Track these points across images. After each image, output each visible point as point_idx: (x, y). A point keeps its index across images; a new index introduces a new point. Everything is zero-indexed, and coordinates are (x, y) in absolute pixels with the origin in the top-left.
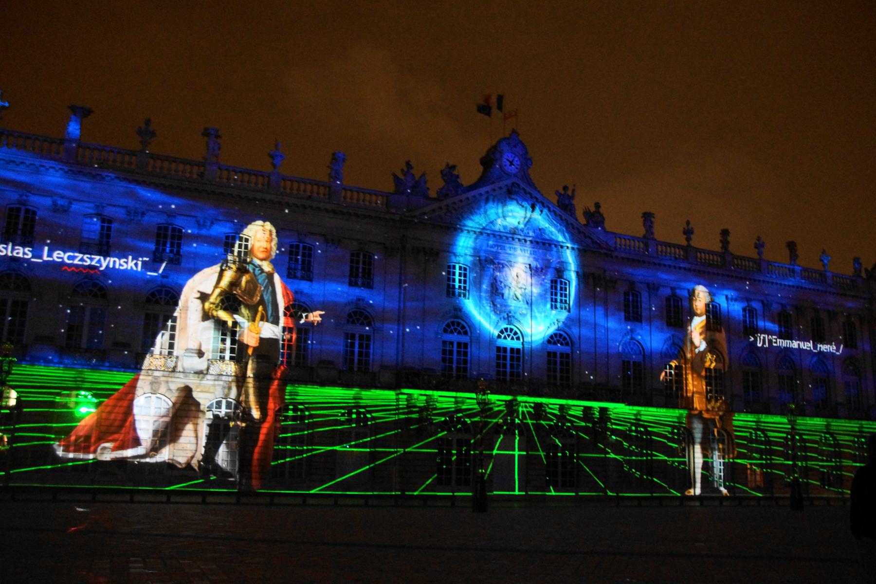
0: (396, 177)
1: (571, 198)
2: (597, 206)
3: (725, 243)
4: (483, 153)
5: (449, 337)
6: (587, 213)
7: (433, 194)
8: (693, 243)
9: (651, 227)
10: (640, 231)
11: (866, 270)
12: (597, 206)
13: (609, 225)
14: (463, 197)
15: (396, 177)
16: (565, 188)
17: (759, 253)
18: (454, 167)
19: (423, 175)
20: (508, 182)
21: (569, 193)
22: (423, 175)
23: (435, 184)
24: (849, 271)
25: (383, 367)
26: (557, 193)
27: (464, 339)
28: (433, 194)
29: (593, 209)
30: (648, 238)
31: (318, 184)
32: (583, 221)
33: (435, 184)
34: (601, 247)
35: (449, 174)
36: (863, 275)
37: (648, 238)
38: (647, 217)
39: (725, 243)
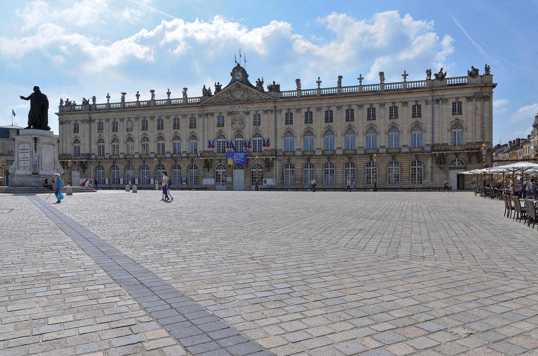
2: (274, 82)
5: (219, 140)
6: (270, 88)
10: (295, 88)
11: (436, 75)
12: (274, 82)
16: (259, 79)
24: (424, 77)
26: (257, 82)
28: (213, 94)
29: (272, 84)
32: (266, 90)
36: (433, 77)
37: (299, 90)
38: (298, 81)
39: (339, 82)
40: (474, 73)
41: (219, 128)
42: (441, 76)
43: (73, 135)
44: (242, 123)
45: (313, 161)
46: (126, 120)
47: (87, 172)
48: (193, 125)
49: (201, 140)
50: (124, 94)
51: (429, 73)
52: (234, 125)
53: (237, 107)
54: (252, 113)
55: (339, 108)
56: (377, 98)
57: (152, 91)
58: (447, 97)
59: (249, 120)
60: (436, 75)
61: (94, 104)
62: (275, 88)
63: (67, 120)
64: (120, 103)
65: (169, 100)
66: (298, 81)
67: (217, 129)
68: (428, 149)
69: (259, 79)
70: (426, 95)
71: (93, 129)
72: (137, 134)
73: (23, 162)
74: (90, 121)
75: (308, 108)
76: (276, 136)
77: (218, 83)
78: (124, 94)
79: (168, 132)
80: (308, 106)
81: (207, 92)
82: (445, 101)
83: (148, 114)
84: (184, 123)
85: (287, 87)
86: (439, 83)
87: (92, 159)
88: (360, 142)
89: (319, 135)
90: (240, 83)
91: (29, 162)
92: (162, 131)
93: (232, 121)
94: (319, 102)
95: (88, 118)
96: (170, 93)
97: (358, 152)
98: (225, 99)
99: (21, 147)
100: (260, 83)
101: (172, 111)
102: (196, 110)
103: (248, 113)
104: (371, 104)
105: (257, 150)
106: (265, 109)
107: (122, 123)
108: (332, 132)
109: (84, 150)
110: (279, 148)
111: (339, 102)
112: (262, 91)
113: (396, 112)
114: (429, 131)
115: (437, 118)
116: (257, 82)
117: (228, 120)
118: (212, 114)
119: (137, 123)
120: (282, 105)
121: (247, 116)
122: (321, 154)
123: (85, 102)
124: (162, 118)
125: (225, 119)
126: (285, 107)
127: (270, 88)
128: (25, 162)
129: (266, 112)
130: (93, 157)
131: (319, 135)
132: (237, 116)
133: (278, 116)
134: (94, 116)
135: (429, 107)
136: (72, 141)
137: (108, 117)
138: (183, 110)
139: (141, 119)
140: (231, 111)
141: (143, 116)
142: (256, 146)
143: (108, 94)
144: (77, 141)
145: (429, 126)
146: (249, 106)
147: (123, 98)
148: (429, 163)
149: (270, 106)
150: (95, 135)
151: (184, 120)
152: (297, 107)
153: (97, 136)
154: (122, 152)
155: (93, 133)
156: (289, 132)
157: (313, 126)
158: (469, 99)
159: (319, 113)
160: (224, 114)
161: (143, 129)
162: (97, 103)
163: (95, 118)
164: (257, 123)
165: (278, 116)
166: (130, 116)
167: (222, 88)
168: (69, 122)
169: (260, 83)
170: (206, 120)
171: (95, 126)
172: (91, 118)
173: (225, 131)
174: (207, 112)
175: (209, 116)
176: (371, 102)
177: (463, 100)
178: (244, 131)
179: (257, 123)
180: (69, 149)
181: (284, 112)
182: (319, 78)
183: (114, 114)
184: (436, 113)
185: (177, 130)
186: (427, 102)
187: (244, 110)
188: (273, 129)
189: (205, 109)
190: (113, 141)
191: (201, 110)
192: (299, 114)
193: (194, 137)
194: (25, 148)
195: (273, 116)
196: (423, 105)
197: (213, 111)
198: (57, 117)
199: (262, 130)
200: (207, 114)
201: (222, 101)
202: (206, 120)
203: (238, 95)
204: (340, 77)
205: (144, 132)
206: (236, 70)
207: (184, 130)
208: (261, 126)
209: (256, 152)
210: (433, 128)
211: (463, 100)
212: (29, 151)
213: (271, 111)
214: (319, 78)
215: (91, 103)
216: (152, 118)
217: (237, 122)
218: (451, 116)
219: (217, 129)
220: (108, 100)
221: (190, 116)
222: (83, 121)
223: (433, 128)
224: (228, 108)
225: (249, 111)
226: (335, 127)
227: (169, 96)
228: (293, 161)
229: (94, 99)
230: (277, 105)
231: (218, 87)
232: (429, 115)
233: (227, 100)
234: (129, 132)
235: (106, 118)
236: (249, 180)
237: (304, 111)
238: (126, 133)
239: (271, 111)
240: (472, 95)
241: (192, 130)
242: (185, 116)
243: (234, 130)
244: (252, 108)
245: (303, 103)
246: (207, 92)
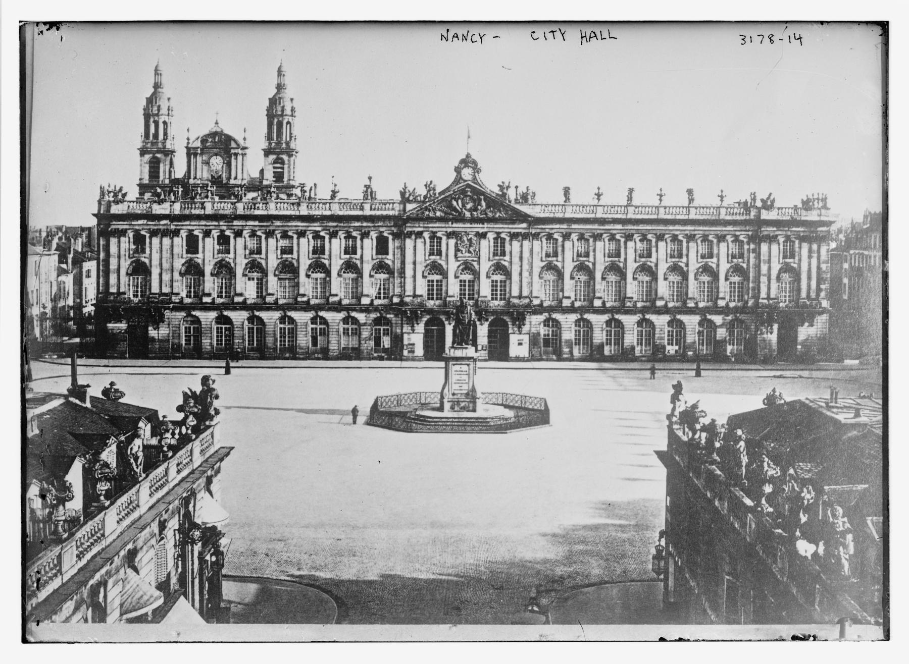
3: (630, 198)
11: (762, 200)
15: (401, 192)
39: (630, 198)
40: (807, 205)
52: (459, 254)
59: (486, 247)
60: (762, 200)
77: (431, 182)
116: (499, 186)
129: (514, 236)
149: (521, 227)
171: (180, 243)
182: (599, 188)
204: (631, 191)
214: (599, 188)
231: (429, 187)
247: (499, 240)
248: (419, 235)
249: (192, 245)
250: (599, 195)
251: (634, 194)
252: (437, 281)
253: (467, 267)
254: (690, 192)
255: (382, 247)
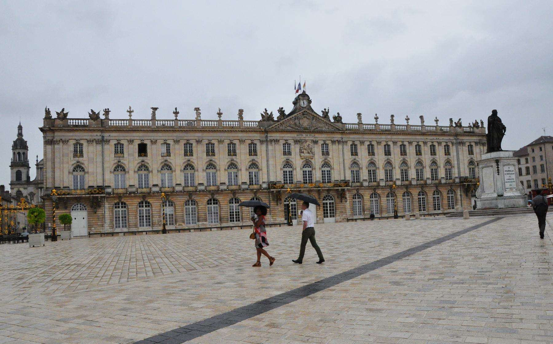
0: (262, 115)
1: (327, 113)
2: (338, 114)
3: (392, 120)
4: (293, 100)
6: (335, 118)
7: (275, 119)
8: (378, 123)
9: (361, 119)
10: (356, 121)
12: (338, 114)
13: (344, 121)
14: (286, 119)
15: (262, 115)
16: (325, 109)
17: (408, 123)
18: (282, 108)
19: (271, 113)
20: (303, 111)
21: (327, 111)
22: (271, 113)
23: (276, 115)
24: (448, 124)
25: (264, 182)
26: (322, 111)
27: (290, 169)
28: (275, 119)
29: (337, 115)
30: (360, 123)
31: (235, 121)
32: (332, 120)
33: (276, 115)
34: (339, 130)
35: (281, 111)
36: (454, 125)
37: (360, 123)
38: (359, 115)
39: (392, 120)
41: (286, 156)
42: (459, 125)
43: (73, 161)
44: (311, 152)
45: (379, 192)
46: (160, 142)
47: (100, 212)
48: (253, 151)
49: (265, 170)
50: (155, 109)
51: (451, 120)
52: (302, 155)
53: (304, 135)
54: (321, 142)
55: (395, 143)
56: (422, 137)
57: (197, 109)
58: (465, 141)
59: (317, 150)
61: (107, 119)
62: (338, 119)
63: (64, 138)
64: (150, 120)
65: (220, 121)
66: (359, 115)
67: (284, 158)
68: (457, 180)
69: (325, 109)
70: (452, 138)
71: (106, 152)
72: (178, 160)
73: (509, 184)
74: (103, 141)
75: (370, 142)
76: (344, 167)
77: (282, 108)
78: (155, 109)
79: (222, 159)
80: (370, 140)
81: (267, 117)
82: (462, 143)
83: (193, 137)
84: (242, 151)
85: (349, 119)
86: (459, 130)
87: (109, 194)
88: (223, 177)
89: (381, 167)
90: (308, 111)
91: (515, 183)
92: (213, 158)
93: (300, 150)
94: (379, 137)
95: (100, 138)
96: (222, 114)
97: (381, 184)
98: (292, 126)
99: (506, 168)
100: (326, 114)
101: (226, 134)
102: (257, 136)
103: (316, 142)
104: (418, 142)
105: (327, 181)
106: (332, 139)
107: (154, 146)
108: (257, 165)
109: (93, 179)
110: (347, 179)
111: (395, 138)
112: (330, 121)
113: (373, 150)
114: (456, 166)
115: (461, 156)
116: (322, 111)
117: (295, 149)
118: (277, 141)
119: (177, 146)
120: (348, 136)
121: (316, 146)
122: (384, 184)
123: (94, 116)
124: (213, 142)
125: (292, 147)
126: (351, 139)
127: (335, 118)
128: (511, 183)
129: (333, 142)
130: (109, 190)
131: (381, 167)
132: (306, 145)
133: (345, 146)
134: (106, 135)
135: (454, 147)
136: (72, 168)
137: (132, 138)
138: (240, 135)
139: (182, 143)
140: (299, 139)
141: (185, 138)
142: (287, 177)
143: (130, 108)
144: (79, 167)
145: (456, 162)
146: (317, 135)
147: (154, 114)
148: (459, 192)
149: (337, 137)
150: (111, 160)
151: (242, 146)
152: (361, 140)
153: (113, 162)
154: (155, 183)
155: (107, 158)
156: (355, 163)
157: (194, 159)
158: (476, 143)
159: (379, 147)
160: (291, 142)
161: (186, 155)
162: (111, 117)
163: (109, 138)
164: (326, 153)
165: (345, 146)
166: (167, 138)
167: (287, 113)
168: (65, 142)
169: (326, 114)
170: (270, 147)
171: (110, 148)
172: (103, 137)
173: (293, 160)
174: (272, 138)
175: (273, 143)
176: (417, 140)
177: (473, 144)
178: (313, 161)
179: (326, 153)
180: (66, 179)
181: (350, 143)
183: (141, 134)
184: (460, 153)
185: (234, 157)
186: (452, 143)
187: (312, 139)
188: (341, 160)
189: (269, 135)
190: (140, 169)
191: (263, 135)
192: (362, 147)
193: (254, 165)
194: (510, 169)
195: (340, 146)
196: (450, 145)
197: (278, 138)
198: (41, 134)
199: (331, 160)
200: (271, 141)
201: (288, 128)
202: (270, 147)
203: (305, 123)
204: (392, 116)
205: (187, 157)
206: (301, 97)
207: (243, 158)
208: (330, 156)
209: (325, 182)
210: (458, 164)
211: (473, 144)
212: (514, 172)
213: (339, 142)
215: (102, 117)
216: (199, 142)
217: (305, 151)
218: (468, 156)
219: (284, 158)
220: (130, 116)
221: (250, 142)
222: (89, 141)
223: (458, 164)
224: (294, 135)
225: (317, 139)
226: (393, 160)
227: (220, 117)
228: (361, 192)
229: (107, 112)
230: (344, 136)
232: (455, 154)
233: (294, 126)
234: (165, 158)
235: (129, 138)
236: (321, 212)
237: (367, 143)
238: (160, 160)
239: (339, 142)
240: (478, 141)
241: (252, 157)
242: (242, 141)
243: (302, 159)
244: (321, 137)
245: (366, 136)
246: (267, 117)
247: (325, 145)
248: (277, 141)
249: (119, 150)
250: (376, 118)
251: (394, 118)
252: (289, 172)
253: (307, 163)
254: (421, 117)
255: (253, 151)
